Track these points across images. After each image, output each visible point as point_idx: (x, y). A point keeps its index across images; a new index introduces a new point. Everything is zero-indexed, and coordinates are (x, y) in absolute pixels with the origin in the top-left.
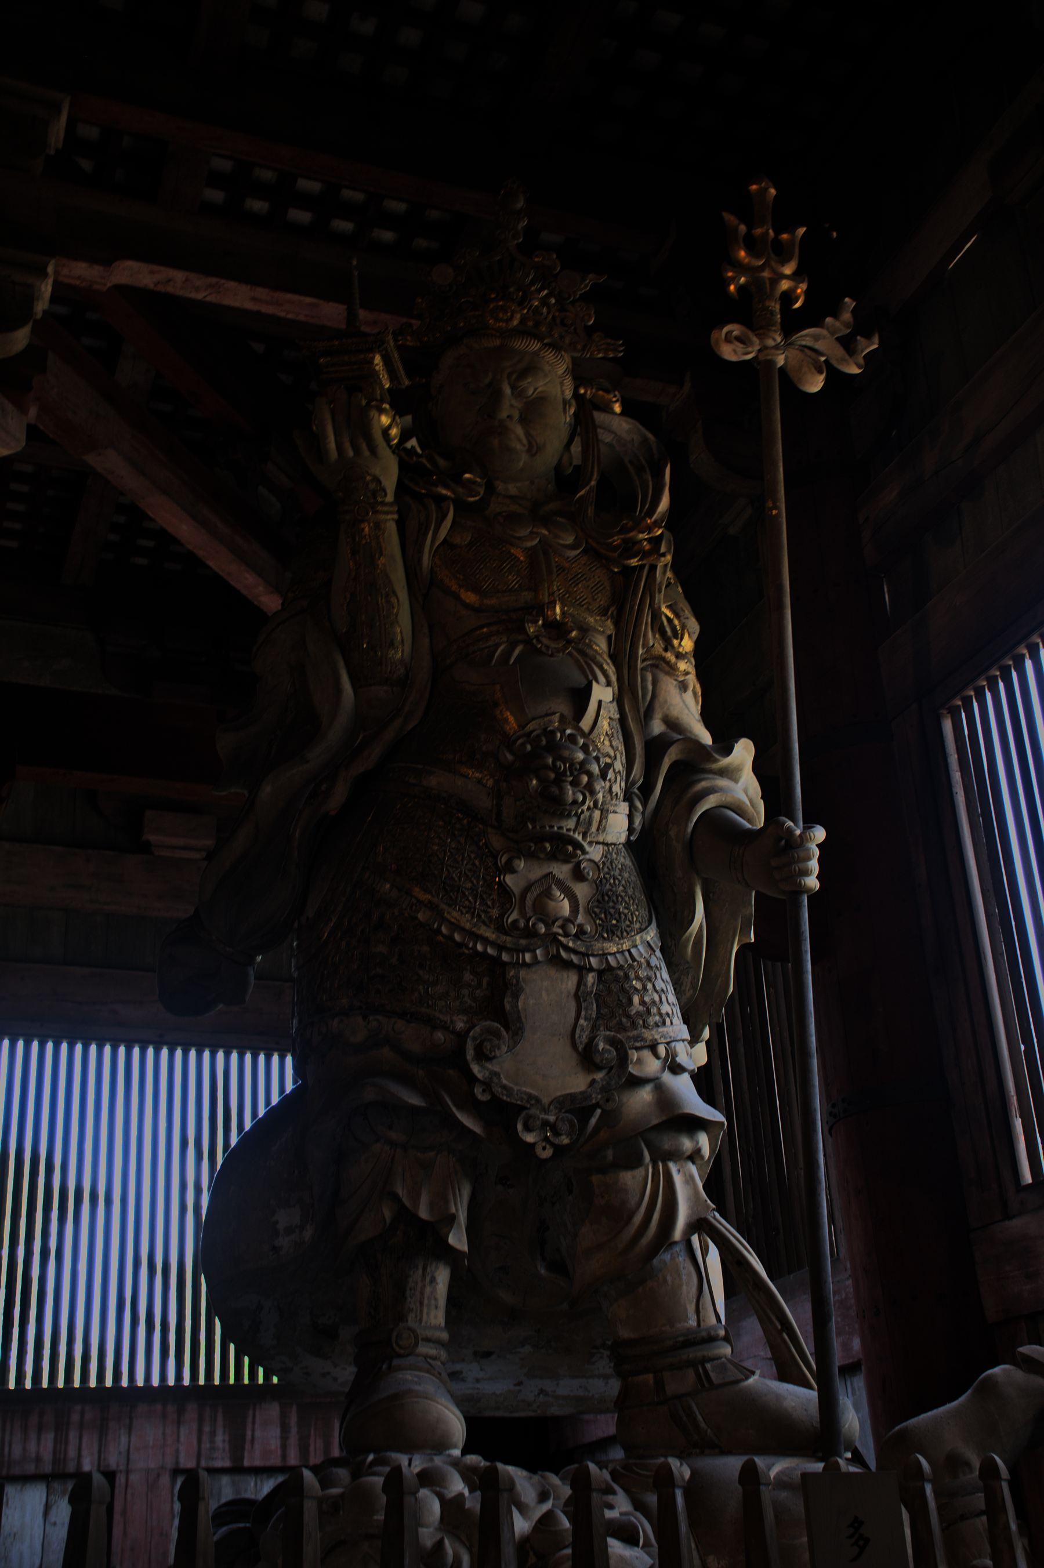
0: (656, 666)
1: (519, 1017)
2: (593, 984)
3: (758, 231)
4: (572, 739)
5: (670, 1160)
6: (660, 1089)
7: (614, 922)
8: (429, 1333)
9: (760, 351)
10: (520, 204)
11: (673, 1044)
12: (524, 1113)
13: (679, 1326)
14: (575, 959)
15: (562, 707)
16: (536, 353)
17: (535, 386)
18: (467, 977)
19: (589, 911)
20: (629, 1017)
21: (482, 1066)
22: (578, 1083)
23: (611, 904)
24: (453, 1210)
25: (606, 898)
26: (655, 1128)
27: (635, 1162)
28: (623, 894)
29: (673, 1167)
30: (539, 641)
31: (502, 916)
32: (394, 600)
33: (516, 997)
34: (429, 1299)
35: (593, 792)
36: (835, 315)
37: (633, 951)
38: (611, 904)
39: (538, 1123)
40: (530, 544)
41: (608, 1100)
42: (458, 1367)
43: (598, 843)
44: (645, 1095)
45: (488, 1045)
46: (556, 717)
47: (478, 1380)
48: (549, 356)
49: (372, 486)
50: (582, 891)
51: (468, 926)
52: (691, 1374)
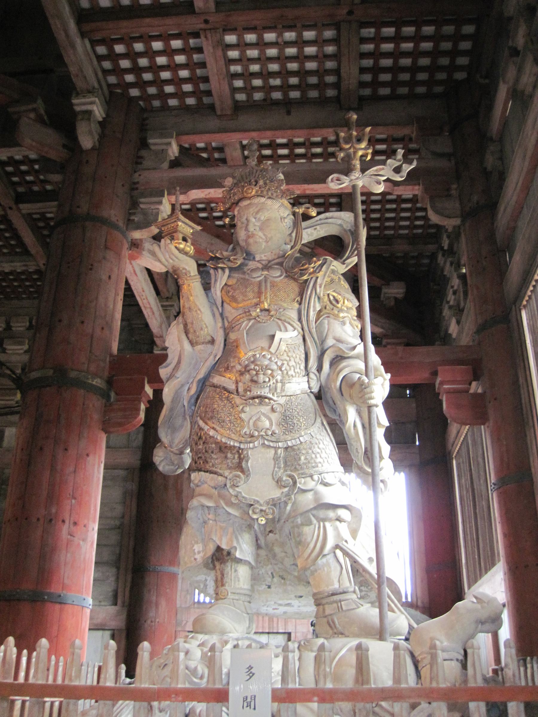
0: (328, 317)
1: (249, 470)
2: (281, 453)
6: (316, 493)
8: (234, 591)
9: (350, 181)
11: (323, 475)
12: (252, 507)
14: (272, 444)
15: (264, 343)
16: (263, 203)
17: (263, 216)
19: (279, 424)
20: (299, 465)
21: (234, 490)
22: (276, 493)
23: (290, 420)
24: (235, 544)
25: (288, 418)
26: (315, 508)
27: (310, 523)
28: (297, 415)
29: (328, 524)
31: (240, 431)
32: (199, 312)
33: (247, 462)
34: (235, 577)
35: (273, 377)
37: (301, 438)
40: (259, 279)
42: (289, 602)
43: (282, 396)
44: (310, 496)
45: (235, 481)
46: (260, 348)
47: (299, 607)
48: (269, 202)
49: (184, 271)
50: (274, 417)
51: (227, 435)
52: (335, 605)
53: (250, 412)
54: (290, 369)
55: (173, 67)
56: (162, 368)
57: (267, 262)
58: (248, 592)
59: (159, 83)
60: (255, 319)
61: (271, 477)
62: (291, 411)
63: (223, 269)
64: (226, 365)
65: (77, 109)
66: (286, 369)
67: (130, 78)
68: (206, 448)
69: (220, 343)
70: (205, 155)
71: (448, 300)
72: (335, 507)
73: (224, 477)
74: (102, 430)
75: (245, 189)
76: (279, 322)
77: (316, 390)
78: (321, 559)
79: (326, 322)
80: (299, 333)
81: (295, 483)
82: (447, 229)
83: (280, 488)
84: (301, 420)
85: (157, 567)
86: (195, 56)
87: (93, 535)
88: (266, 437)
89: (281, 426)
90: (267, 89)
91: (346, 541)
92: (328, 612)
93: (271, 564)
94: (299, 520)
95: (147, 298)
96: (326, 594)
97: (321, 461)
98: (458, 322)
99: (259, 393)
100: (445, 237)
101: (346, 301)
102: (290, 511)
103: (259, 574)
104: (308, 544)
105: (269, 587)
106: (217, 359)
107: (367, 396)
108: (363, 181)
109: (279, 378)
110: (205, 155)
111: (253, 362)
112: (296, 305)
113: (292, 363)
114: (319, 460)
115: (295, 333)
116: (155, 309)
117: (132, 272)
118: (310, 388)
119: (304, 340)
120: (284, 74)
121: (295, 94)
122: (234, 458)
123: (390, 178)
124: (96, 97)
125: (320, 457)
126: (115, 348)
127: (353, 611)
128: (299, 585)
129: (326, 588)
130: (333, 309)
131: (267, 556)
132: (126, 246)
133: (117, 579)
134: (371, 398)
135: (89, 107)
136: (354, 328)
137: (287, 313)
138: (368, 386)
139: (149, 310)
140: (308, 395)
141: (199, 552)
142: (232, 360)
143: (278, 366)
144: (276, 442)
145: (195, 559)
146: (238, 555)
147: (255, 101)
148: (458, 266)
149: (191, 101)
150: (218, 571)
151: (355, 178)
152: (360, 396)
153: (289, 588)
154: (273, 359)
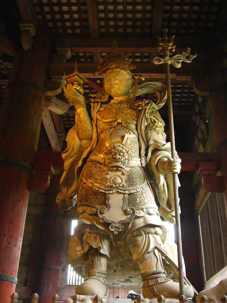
0: (151, 130)
3: (164, 38)
4: (119, 146)
5: (149, 234)
6: (145, 218)
7: (132, 183)
8: (99, 272)
9: (164, 61)
10: (115, 44)
11: (148, 209)
13: (151, 270)
14: (122, 192)
15: (119, 139)
16: (119, 71)
18: (99, 197)
19: (126, 181)
21: (101, 215)
22: (124, 218)
24: (101, 246)
25: (131, 178)
26: (144, 227)
27: (141, 235)
28: (135, 177)
29: (150, 236)
30: (116, 127)
31: (105, 184)
33: (109, 200)
34: (99, 264)
35: (124, 156)
36: (186, 52)
38: (132, 180)
39: (114, 227)
40: (116, 108)
41: (131, 221)
44: (141, 220)
45: (102, 211)
48: (122, 71)
50: (124, 177)
51: (98, 186)
53: (111, 175)
54: (132, 153)
55: (70, 12)
56: (63, 153)
57: (120, 101)
58: (106, 273)
59: (63, 20)
60: (114, 128)
61: (121, 210)
62: (132, 175)
63: (98, 102)
64: (99, 150)
65: (22, 29)
66: (130, 153)
67: (49, 17)
68: (87, 193)
69: (96, 140)
70: (83, 60)
71: (198, 136)
72: (154, 226)
73: (96, 208)
74: (28, 189)
75: (110, 64)
76: (127, 130)
77: (144, 165)
78: (147, 254)
79: (149, 132)
80: (136, 136)
81: (134, 212)
82: (199, 102)
83: (126, 215)
84: (137, 180)
85: (49, 266)
86: (82, 7)
87: (20, 244)
88: (119, 188)
89: (127, 182)
90: (116, 27)
91: (160, 245)
92: (150, 284)
93: (117, 259)
94: (135, 233)
95: (51, 130)
96: (149, 274)
97: (148, 201)
98: (204, 147)
99: (116, 165)
100: (197, 106)
101: (159, 123)
102: (131, 228)
103: (110, 264)
104: (140, 246)
105: (115, 272)
106: (93, 148)
107: (173, 168)
108: (171, 62)
109: (127, 157)
110: (83, 60)
111: (113, 148)
112: (135, 122)
113: (133, 150)
114: (146, 201)
115: (135, 136)
116: (54, 136)
117: (45, 115)
118: (141, 164)
119: (139, 140)
120: (125, 19)
121: (129, 31)
122: (102, 198)
123: (184, 61)
124: (32, 23)
125: (147, 199)
126: (36, 148)
127: (165, 283)
128: (131, 270)
129: (149, 271)
130: (153, 126)
131: (115, 254)
132: (44, 99)
133: (28, 272)
134: (175, 169)
135: (28, 29)
136: (163, 136)
137: (131, 126)
138: (173, 162)
139: (51, 136)
140: (140, 168)
141: (79, 251)
142: (102, 147)
143: (126, 151)
144: (124, 191)
145: (77, 255)
146: (102, 251)
147: (110, 33)
148: (204, 120)
149: (78, 31)
150: (90, 261)
151: (167, 59)
152: (169, 168)
153: (126, 272)
154: (124, 147)
